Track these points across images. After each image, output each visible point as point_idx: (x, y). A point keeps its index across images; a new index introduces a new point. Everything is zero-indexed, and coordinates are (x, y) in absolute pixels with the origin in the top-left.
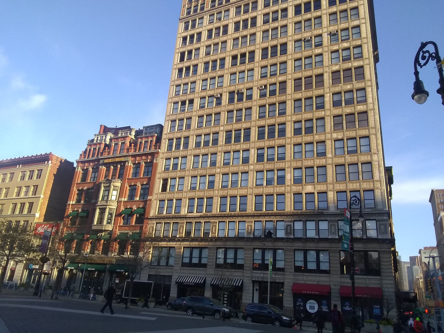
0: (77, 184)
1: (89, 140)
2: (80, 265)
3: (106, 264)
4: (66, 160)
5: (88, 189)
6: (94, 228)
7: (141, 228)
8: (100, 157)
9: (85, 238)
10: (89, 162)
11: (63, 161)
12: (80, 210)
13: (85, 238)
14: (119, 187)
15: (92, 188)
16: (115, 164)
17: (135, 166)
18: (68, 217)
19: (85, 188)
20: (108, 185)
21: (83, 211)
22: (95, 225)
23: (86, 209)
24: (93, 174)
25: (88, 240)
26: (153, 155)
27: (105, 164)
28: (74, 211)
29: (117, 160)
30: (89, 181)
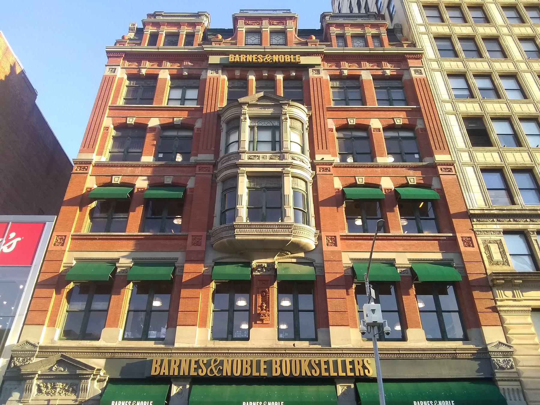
0: (112, 108)
2: (175, 389)
3: (331, 381)
4: (23, 72)
5: (165, 127)
6: (240, 235)
7: (450, 245)
8: (207, 48)
9: (186, 278)
10: (159, 58)
11: (18, 71)
12: (141, 183)
13: (186, 278)
14: (306, 126)
15: (184, 126)
16: (266, 70)
17: (337, 84)
18: (82, 201)
19: (154, 122)
20: (269, 111)
21: (152, 186)
22: (245, 226)
23: (168, 180)
24: (177, 94)
25: (201, 282)
26: (400, 60)
27: (225, 67)
28: (110, 184)
30: (164, 104)
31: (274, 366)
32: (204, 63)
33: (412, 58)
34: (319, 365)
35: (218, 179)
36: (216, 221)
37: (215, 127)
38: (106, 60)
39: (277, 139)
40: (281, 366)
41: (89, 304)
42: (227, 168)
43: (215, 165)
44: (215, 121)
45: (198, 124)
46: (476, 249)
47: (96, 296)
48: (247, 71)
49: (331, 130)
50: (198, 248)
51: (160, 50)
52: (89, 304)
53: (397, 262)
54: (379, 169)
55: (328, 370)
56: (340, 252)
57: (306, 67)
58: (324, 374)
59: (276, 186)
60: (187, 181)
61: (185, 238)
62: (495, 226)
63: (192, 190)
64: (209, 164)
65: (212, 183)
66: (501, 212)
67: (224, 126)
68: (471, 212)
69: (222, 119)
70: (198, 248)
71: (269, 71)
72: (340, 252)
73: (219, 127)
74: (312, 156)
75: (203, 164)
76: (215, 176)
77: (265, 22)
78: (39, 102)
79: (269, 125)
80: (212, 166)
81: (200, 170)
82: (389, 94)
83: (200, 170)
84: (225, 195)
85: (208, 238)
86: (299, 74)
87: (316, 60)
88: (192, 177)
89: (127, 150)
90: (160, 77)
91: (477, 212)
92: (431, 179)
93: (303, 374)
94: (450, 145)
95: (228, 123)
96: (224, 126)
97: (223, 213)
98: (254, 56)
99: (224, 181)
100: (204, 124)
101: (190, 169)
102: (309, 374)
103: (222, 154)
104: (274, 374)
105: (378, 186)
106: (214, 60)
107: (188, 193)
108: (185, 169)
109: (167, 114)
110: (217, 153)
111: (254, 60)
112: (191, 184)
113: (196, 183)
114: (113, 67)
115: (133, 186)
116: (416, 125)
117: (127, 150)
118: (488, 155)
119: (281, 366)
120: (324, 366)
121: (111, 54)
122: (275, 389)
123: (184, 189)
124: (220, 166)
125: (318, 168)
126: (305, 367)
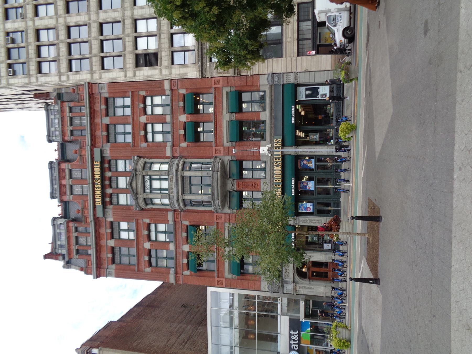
1: (64, 267)
29: (97, 176)
31: (278, 181)
32: (100, 219)
33: (92, 90)
34: (277, 162)
35: (184, 209)
36: (208, 209)
37: (149, 212)
38: (102, 278)
39: (158, 177)
40: (277, 179)
41: (250, 264)
42: (179, 205)
43: (175, 211)
44: (145, 212)
45: (147, 221)
46: (221, 79)
47: (245, 261)
48: (105, 193)
49: (148, 146)
50: (223, 217)
51: (94, 247)
52: (250, 264)
53: (228, 119)
54: (174, 121)
55: (279, 159)
56: (224, 147)
57: (102, 158)
58: (280, 160)
59: (189, 179)
60: (184, 225)
61: (217, 224)
62: (208, 65)
63: (190, 222)
64: (174, 214)
65: (186, 212)
66: (200, 61)
67: (149, 207)
68: (200, 77)
69: (143, 208)
70: (223, 217)
71: (105, 180)
72: (224, 147)
73: (148, 210)
74: (168, 158)
75: (174, 217)
76: (182, 211)
77: (64, 182)
78: (116, 319)
79: (149, 182)
80: (176, 213)
81: (178, 219)
82: (120, 107)
83: (178, 219)
84: (194, 205)
85: (217, 212)
86: (106, 162)
87: (97, 152)
88: (183, 222)
89: (164, 258)
90: (113, 245)
91: (201, 74)
92: (180, 94)
93: (280, 169)
94: (157, 78)
95: (147, 204)
96: (149, 207)
97: (204, 206)
98: (96, 189)
99: (185, 205)
100: (147, 218)
101: (177, 224)
102: (281, 167)
103: (168, 207)
104: (281, 181)
105: (185, 123)
106: (99, 214)
107: (192, 224)
108: (177, 227)
109: (141, 239)
110: (167, 210)
111: (100, 190)
112: (186, 223)
113: (186, 220)
114: (108, 273)
115: (188, 252)
116: (144, 96)
117: (164, 258)
118: (163, 58)
119: (277, 179)
120: (277, 160)
121: (98, 276)
122: (287, 182)
123: (189, 227)
124: (177, 207)
125: (174, 155)
126: (278, 168)
